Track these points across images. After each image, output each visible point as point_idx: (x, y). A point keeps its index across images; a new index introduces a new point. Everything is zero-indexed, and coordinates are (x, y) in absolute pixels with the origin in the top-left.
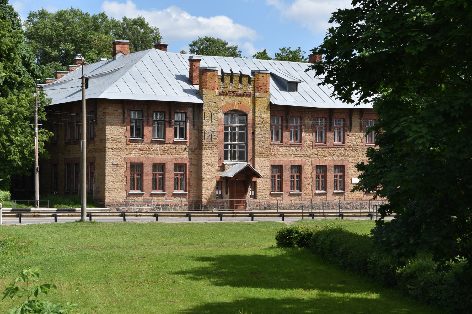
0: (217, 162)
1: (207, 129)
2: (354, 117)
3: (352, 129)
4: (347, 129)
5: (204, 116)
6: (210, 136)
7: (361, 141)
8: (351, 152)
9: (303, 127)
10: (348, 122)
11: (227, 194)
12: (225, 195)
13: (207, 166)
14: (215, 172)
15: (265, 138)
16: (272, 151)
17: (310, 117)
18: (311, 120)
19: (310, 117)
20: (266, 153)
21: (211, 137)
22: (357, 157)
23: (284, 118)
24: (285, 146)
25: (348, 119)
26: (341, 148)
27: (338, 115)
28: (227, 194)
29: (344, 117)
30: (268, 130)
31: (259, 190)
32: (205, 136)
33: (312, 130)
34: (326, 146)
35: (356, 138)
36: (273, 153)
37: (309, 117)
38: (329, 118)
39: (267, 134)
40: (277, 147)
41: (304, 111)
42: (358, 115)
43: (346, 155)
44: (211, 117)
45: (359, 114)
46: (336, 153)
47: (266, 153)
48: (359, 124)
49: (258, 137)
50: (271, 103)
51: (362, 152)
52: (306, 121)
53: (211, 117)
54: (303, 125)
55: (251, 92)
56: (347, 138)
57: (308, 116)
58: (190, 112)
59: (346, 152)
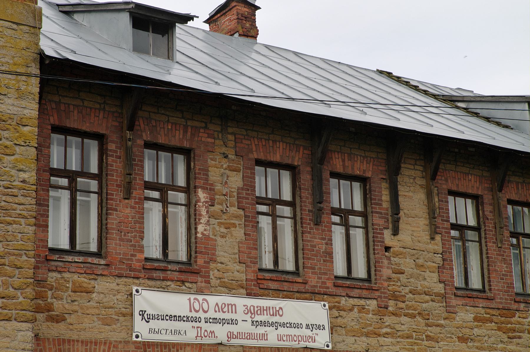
2: (406, 179)
3: (402, 225)
4: (382, 222)
7: (435, 276)
8: (404, 319)
9: (202, 195)
10: (385, 196)
15: (8, 219)
16: (53, 297)
18: (237, 170)
19: (232, 157)
20: (14, 298)
22: (425, 343)
23: (112, 146)
24: (120, 276)
25: (385, 185)
26: (362, 302)
27: (343, 161)
29: (369, 174)
30: (24, 181)
33: (241, 212)
34: (301, 288)
35: (420, 261)
36: (57, 304)
38: (309, 169)
39: (21, 199)
40: (76, 277)
41: (206, 128)
42: (419, 173)
43: (384, 330)
45: (421, 168)
46: (345, 321)
47: (14, 298)
48: (425, 209)
50: (42, 57)
51: (442, 322)
52: (214, 175)
54: (203, 188)
56: (386, 262)
57: (224, 150)
59: (386, 318)
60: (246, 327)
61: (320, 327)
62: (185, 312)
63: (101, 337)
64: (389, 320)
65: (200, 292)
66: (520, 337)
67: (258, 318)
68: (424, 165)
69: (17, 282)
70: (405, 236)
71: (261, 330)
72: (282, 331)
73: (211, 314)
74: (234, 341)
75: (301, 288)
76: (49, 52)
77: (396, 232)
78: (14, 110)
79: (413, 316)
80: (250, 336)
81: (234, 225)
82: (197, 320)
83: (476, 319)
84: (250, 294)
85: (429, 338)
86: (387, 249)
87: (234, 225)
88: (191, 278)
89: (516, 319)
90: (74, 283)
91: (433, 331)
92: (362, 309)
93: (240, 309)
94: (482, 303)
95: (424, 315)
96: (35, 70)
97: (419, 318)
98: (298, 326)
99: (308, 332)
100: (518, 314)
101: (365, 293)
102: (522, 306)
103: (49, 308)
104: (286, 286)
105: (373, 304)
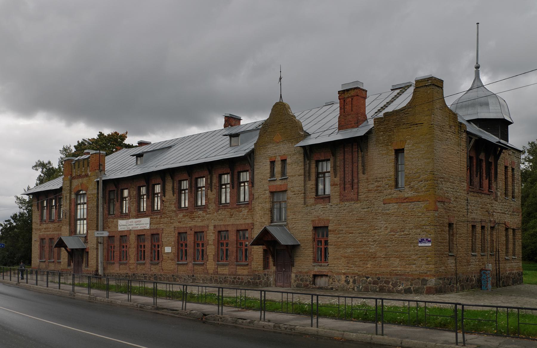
3: (167, 194)
8: (166, 219)
17: (134, 187)
22: (170, 224)
26: (157, 216)
37: (133, 188)
51: (174, 218)
60: (134, 226)
61: (148, 224)
62: (125, 224)
63: (114, 230)
64: (162, 220)
65: (128, 219)
66: (195, 219)
67: (137, 223)
68: (145, 184)
70: (167, 197)
71: (137, 226)
72: (141, 225)
73: (129, 224)
74: (133, 229)
75: (145, 215)
77: (165, 196)
79: (168, 218)
80: (135, 228)
81: (134, 203)
82: (127, 225)
83: (183, 216)
84: (136, 218)
85: (171, 223)
86: (164, 201)
87: (134, 203)
88: (127, 216)
89: (194, 214)
91: (172, 221)
92: (157, 218)
93: (134, 222)
94: (184, 211)
95: (171, 217)
97: (169, 218)
98: (144, 224)
99: (145, 225)
100: (195, 213)
101: (157, 214)
102: (196, 210)
104: (142, 215)
105: (159, 216)
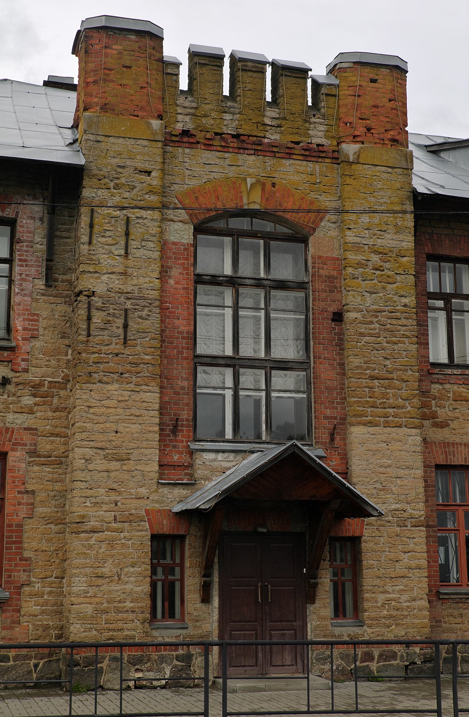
0: (156, 444)
1: (100, 289)
5: (91, 226)
6: (120, 322)
11: (206, 599)
12: (199, 605)
13: (99, 464)
14: (143, 491)
15: (394, 339)
20: (403, 407)
21: (126, 326)
28: (206, 599)
30: (405, 306)
31: (377, 582)
32: (95, 320)
36: (441, 412)
39: (404, 322)
40: (456, 387)
44: (127, 234)
49: (362, 335)
50: (415, 194)
53: (127, 234)
55: (324, 141)
58: (33, 218)
69: (405, 393)
76: (421, 189)
78: (393, 244)
90: (454, 393)
96: (410, 207)
103: (434, 416)
